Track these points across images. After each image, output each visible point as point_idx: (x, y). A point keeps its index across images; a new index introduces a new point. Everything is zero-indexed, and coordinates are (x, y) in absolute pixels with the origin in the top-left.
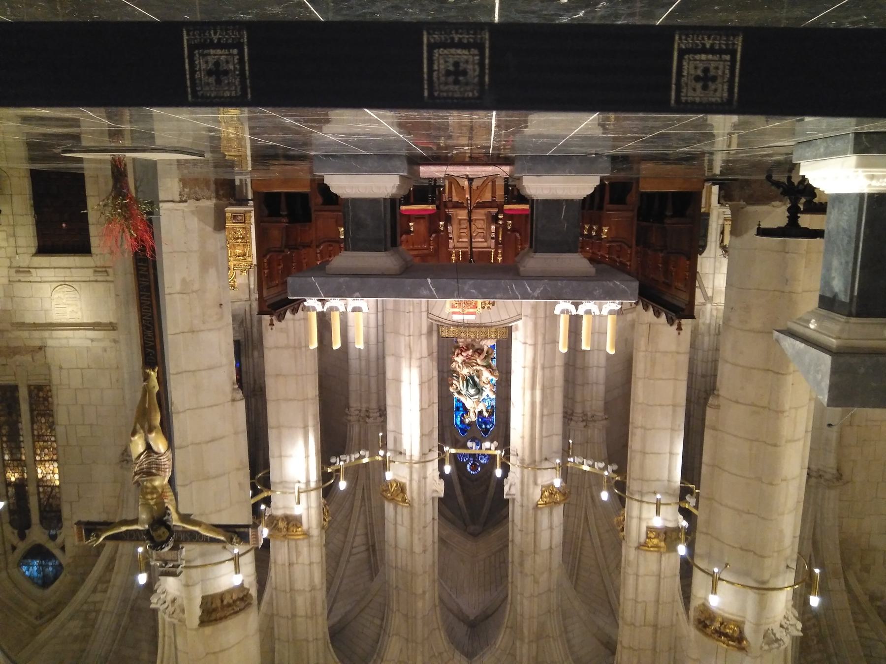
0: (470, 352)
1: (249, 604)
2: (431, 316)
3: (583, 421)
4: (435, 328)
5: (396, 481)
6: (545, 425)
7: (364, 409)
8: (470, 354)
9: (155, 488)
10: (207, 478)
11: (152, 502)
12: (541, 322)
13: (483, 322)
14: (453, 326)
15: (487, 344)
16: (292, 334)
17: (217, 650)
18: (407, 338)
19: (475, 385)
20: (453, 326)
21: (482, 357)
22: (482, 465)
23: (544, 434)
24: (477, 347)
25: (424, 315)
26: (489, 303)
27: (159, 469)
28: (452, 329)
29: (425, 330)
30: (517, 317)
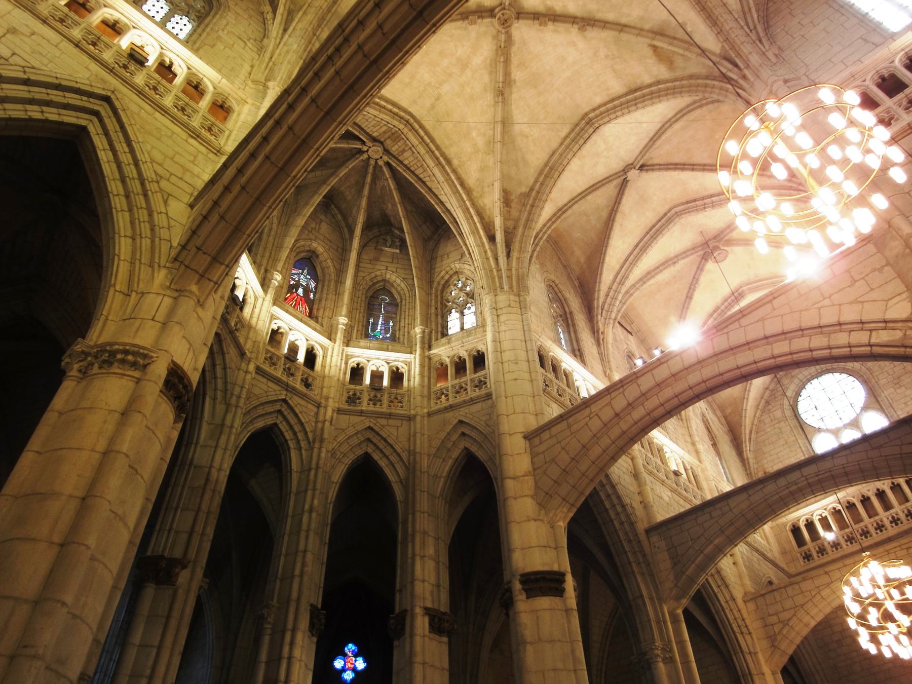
5: (313, 635)
6: (150, 663)
17: (548, 549)
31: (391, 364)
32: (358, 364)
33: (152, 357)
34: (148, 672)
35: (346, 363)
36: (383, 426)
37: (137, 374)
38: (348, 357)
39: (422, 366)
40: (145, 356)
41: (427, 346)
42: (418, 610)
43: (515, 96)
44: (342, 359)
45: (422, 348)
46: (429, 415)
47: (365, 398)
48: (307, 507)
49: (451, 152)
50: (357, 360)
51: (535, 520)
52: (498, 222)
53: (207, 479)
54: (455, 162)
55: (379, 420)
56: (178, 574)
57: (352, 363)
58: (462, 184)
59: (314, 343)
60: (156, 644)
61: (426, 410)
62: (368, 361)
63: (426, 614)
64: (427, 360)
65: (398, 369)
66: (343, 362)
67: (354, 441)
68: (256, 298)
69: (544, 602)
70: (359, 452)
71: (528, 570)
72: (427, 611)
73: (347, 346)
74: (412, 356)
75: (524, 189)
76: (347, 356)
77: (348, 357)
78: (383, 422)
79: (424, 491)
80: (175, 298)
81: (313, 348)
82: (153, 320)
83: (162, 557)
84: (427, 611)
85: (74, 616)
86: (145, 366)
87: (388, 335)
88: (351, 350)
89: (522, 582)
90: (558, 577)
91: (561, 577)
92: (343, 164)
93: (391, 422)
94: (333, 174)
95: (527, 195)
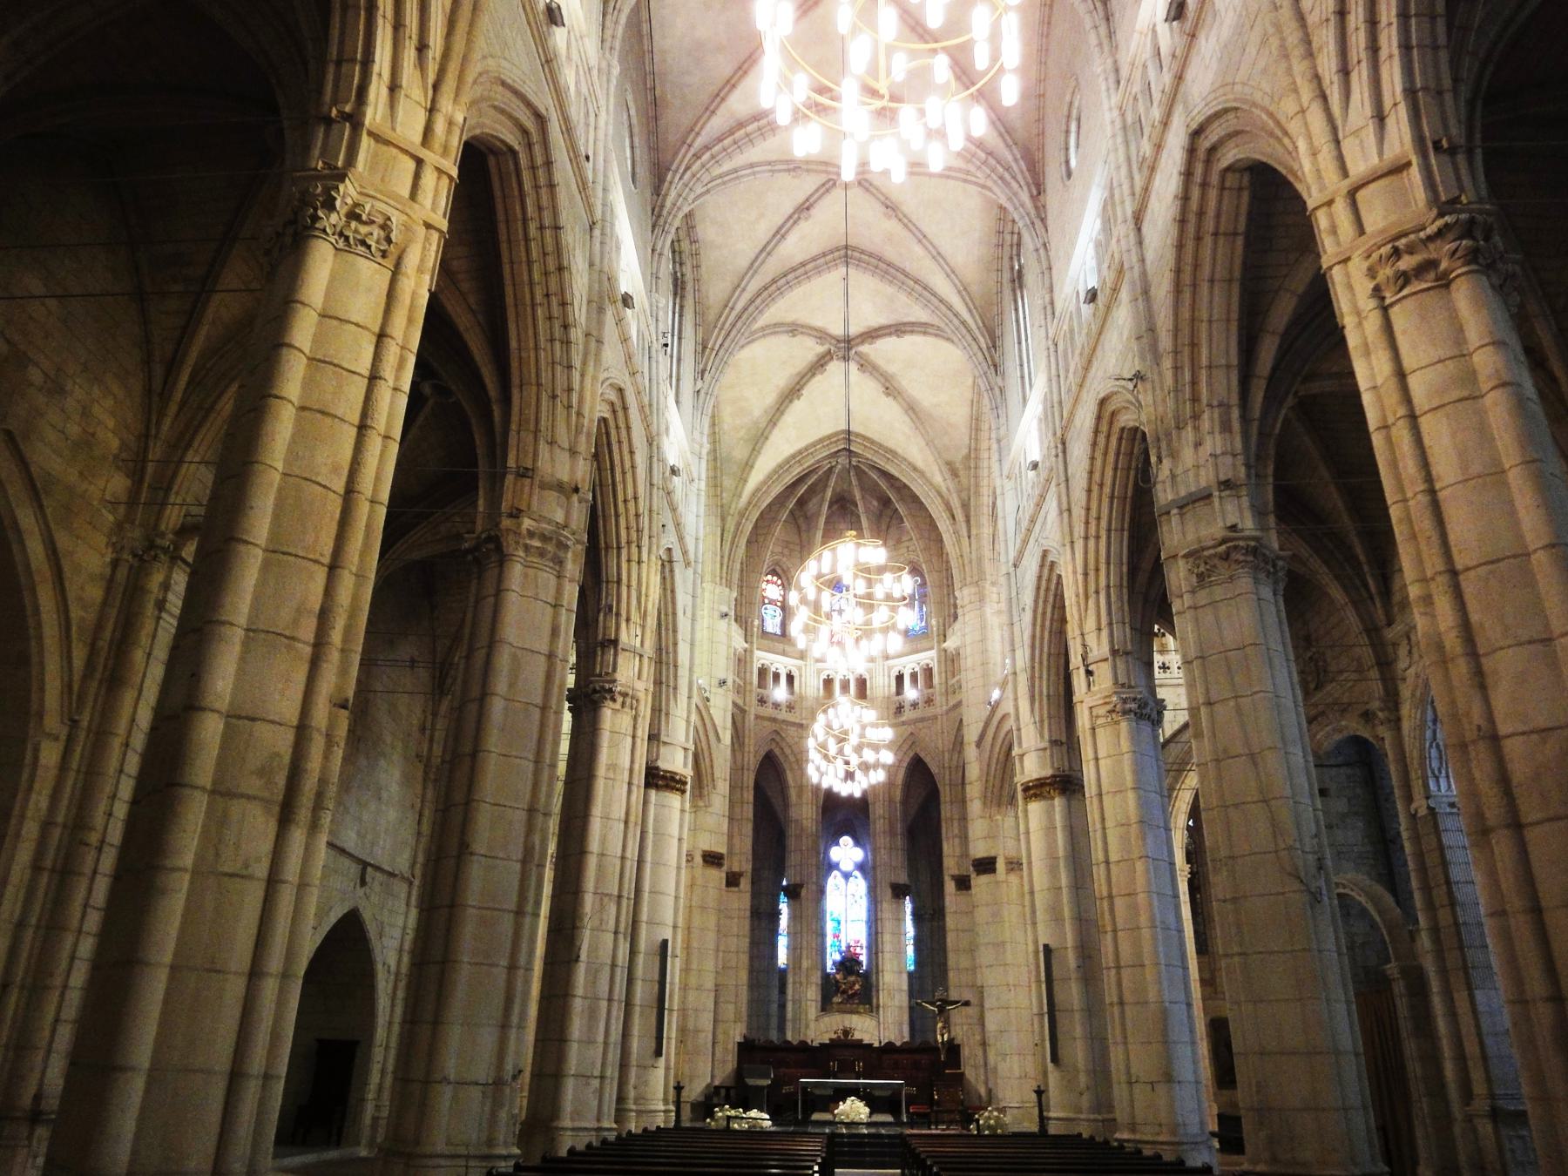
12: (803, 1017)
15: (837, 999)
38: (890, 669)
39: (939, 662)
43: (904, 383)
45: (939, 642)
46: (948, 712)
47: (907, 707)
49: (890, 444)
52: (955, 503)
54: (900, 451)
57: (894, 673)
58: (915, 469)
61: (945, 708)
68: (800, 669)
70: (912, 754)
75: (965, 451)
78: (920, 725)
92: (826, 486)
93: (925, 724)
94: (823, 499)
95: (968, 457)
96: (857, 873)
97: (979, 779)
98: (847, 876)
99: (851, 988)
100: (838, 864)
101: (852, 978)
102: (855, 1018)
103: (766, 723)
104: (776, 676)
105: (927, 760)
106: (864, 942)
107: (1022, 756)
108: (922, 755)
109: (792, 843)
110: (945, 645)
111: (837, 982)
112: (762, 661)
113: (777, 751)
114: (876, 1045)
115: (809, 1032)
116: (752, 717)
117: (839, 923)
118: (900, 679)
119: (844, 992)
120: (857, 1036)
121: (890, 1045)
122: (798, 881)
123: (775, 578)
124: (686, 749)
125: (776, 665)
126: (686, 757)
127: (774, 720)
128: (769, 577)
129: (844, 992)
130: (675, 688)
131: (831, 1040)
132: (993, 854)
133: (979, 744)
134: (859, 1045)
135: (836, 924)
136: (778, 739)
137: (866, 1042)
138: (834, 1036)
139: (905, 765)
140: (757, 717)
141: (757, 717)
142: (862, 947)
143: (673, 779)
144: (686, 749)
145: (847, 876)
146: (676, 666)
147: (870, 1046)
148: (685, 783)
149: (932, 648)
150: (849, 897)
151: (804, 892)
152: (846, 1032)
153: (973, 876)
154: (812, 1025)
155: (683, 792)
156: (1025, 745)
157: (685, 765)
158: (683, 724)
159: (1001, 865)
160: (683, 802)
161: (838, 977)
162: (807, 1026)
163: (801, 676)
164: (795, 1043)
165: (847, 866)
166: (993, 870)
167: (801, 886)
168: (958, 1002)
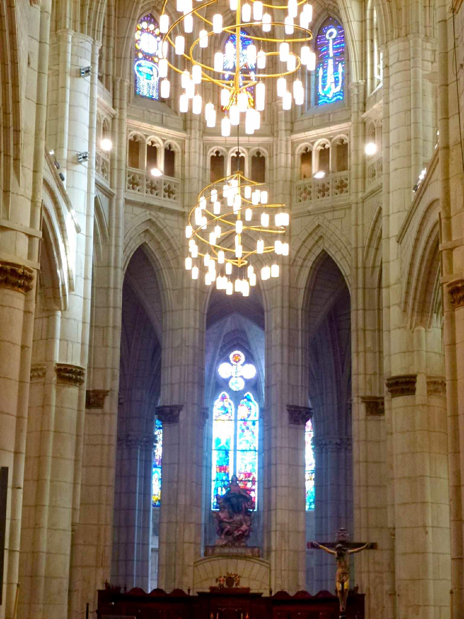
0: (236, 533)
1: (388, 380)
2: (268, 566)
3: (130, 441)
4: (265, 554)
7: (343, 450)
8: (236, 532)
9: (342, 568)
10: (409, 478)
11: (343, 563)
13: (225, 561)
14: (249, 557)
16: (371, 561)
17: (407, 354)
18: (287, 548)
19: (232, 506)
20: (249, 557)
21: (226, 530)
22: (228, 360)
23: (176, 466)
24: (230, 538)
25: (273, 568)
26: (220, 581)
27: (340, 575)
28: (250, 555)
29: (273, 554)
30: (197, 564)
31: (333, 140)
32: (307, 149)
33: (45, 369)
34: (176, 479)
35: (293, 154)
36: (329, 221)
37: (42, 380)
38: (294, 144)
40: (42, 369)
41: (361, 105)
42: (355, 399)
44: (287, 154)
46: (364, 200)
48: (273, 325)
50: (303, 145)
51: (399, 328)
53: (182, 339)
55: (326, 215)
56: (178, 415)
57: (300, 149)
59: (257, 148)
60: (176, 462)
61: (360, 195)
62: (313, 143)
63: (362, 402)
64: (361, 126)
65: (342, 141)
66: (290, 156)
67: (310, 243)
69: (399, 401)
70: (318, 251)
71: (394, 374)
72: (365, 399)
73: (292, 131)
74: (350, 123)
76: (293, 143)
77: (294, 144)
78: (329, 216)
79: (359, 288)
80: (48, 317)
81: (258, 153)
82: (41, 339)
83: (164, 407)
84: (365, 399)
85: (53, 507)
86: (44, 374)
87: (339, 88)
88: (297, 137)
89: (388, 385)
90: (408, 379)
91: (412, 379)
93: (337, 214)
96: (250, 395)
97: (399, 281)
98: (237, 397)
99: (237, 529)
100: (227, 381)
101: (238, 518)
102: (241, 564)
103: (138, 210)
104: (152, 151)
105: (337, 258)
106: (255, 475)
107: (452, 250)
108: (332, 252)
109: (167, 355)
110: (364, 115)
111: (221, 521)
112: (134, 132)
113: (152, 246)
114: (266, 594)
115: (185, 579)
116: (122, 202)
117: (227, 452)
118: (306, 156)
119: (228, 533)
120: (244, 584)
121: (282, 594)
122: (176, 402)
123: (152, 27)
124: (30, 237)
125: (152, 137)
126: (30, 246)
127: (147, 206)
128: (144, 25)
129: (228, 533)
130: (17, 159)
131: (212, 588)
132: (411, 373)
133: (400, 239)
134: (245, 594)
135: (222, 454)
136: (152, 231)
137: (254, 590)
138: (215, 585)
139: (310, 264)
140: (127, 202)
141: (128, 202)
142: (253, 481)
143: (14, 272)
144: (30, 237)
145: (237, 397)
146: (17, 131)
147: (259, 595)
148: (30, 278)
149: (348, 120)
150: (240, 423)
151: (182, 416)
152: (230, 580)
153: (387, 397)
154: (190, 571)
155: (27, 289)
156: (454, 238)
157: (30, 256)
158: (28, 205)
159: (421, 385)
160: (27, 301)
161: (222, 515)
162: (184, 573)
163: (183, 152)
164: (168, 592)
165: (237, 385)
166: (412, 391)
167: (179, 408)
168: (362, 544)
